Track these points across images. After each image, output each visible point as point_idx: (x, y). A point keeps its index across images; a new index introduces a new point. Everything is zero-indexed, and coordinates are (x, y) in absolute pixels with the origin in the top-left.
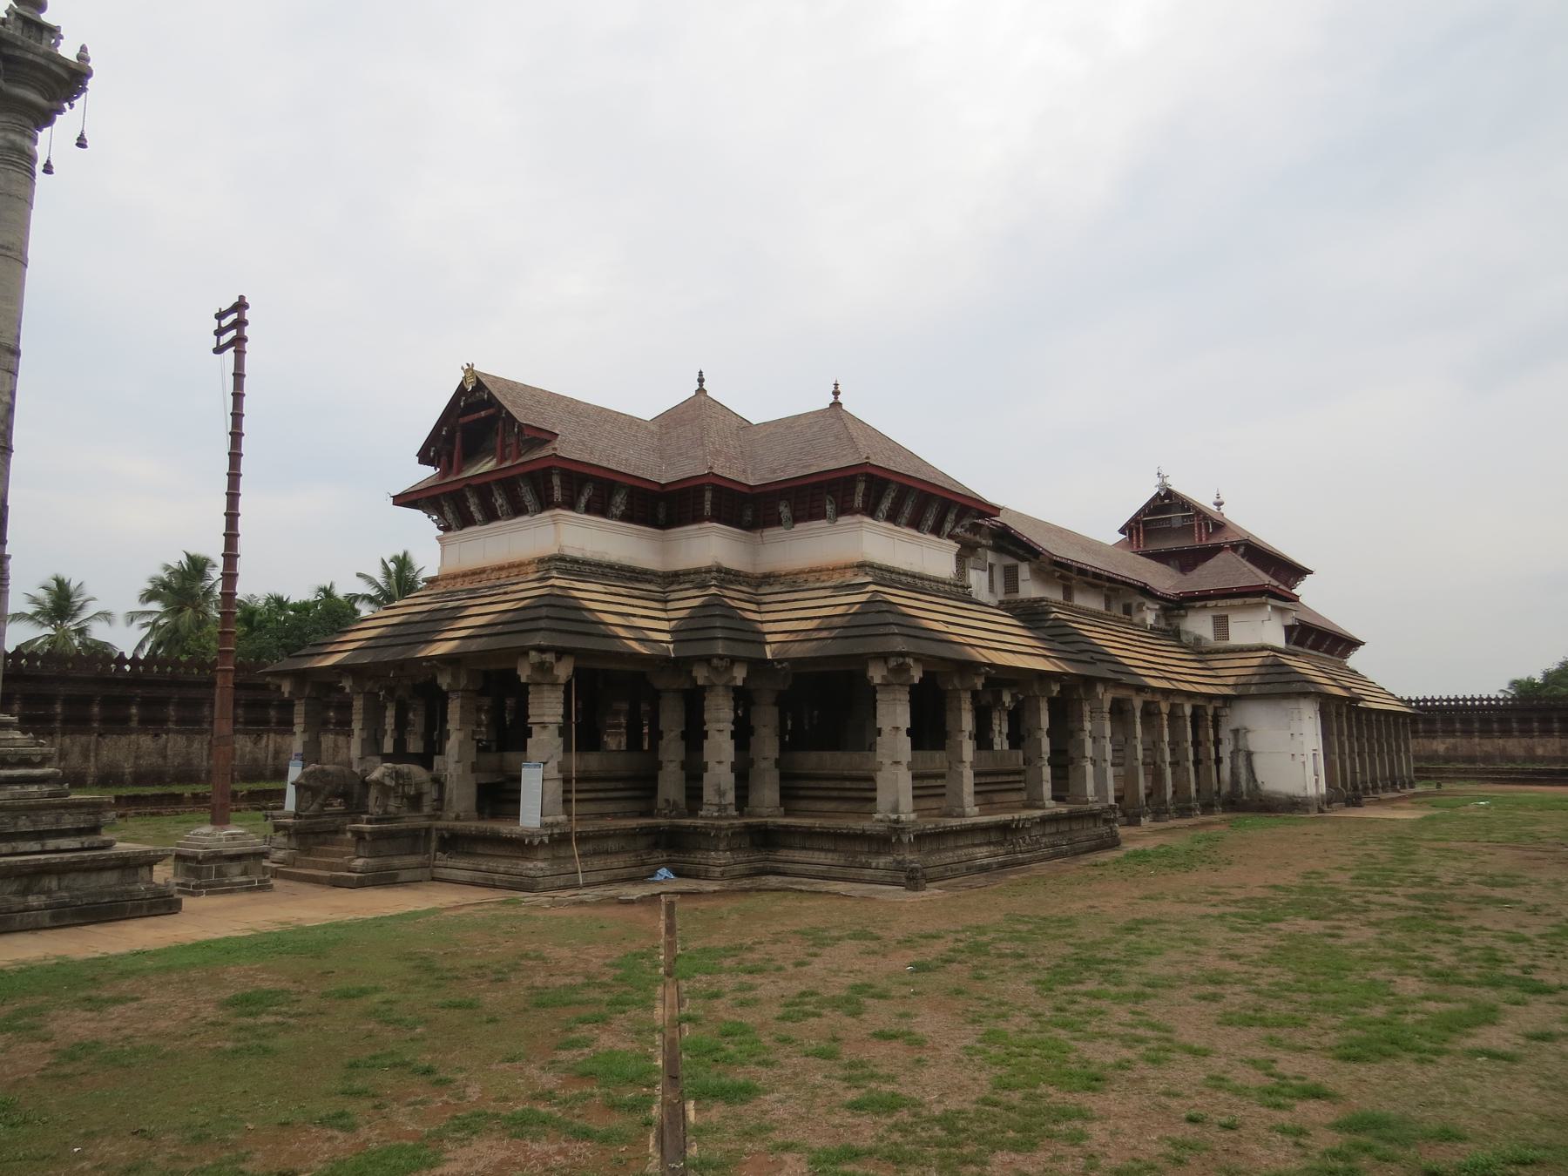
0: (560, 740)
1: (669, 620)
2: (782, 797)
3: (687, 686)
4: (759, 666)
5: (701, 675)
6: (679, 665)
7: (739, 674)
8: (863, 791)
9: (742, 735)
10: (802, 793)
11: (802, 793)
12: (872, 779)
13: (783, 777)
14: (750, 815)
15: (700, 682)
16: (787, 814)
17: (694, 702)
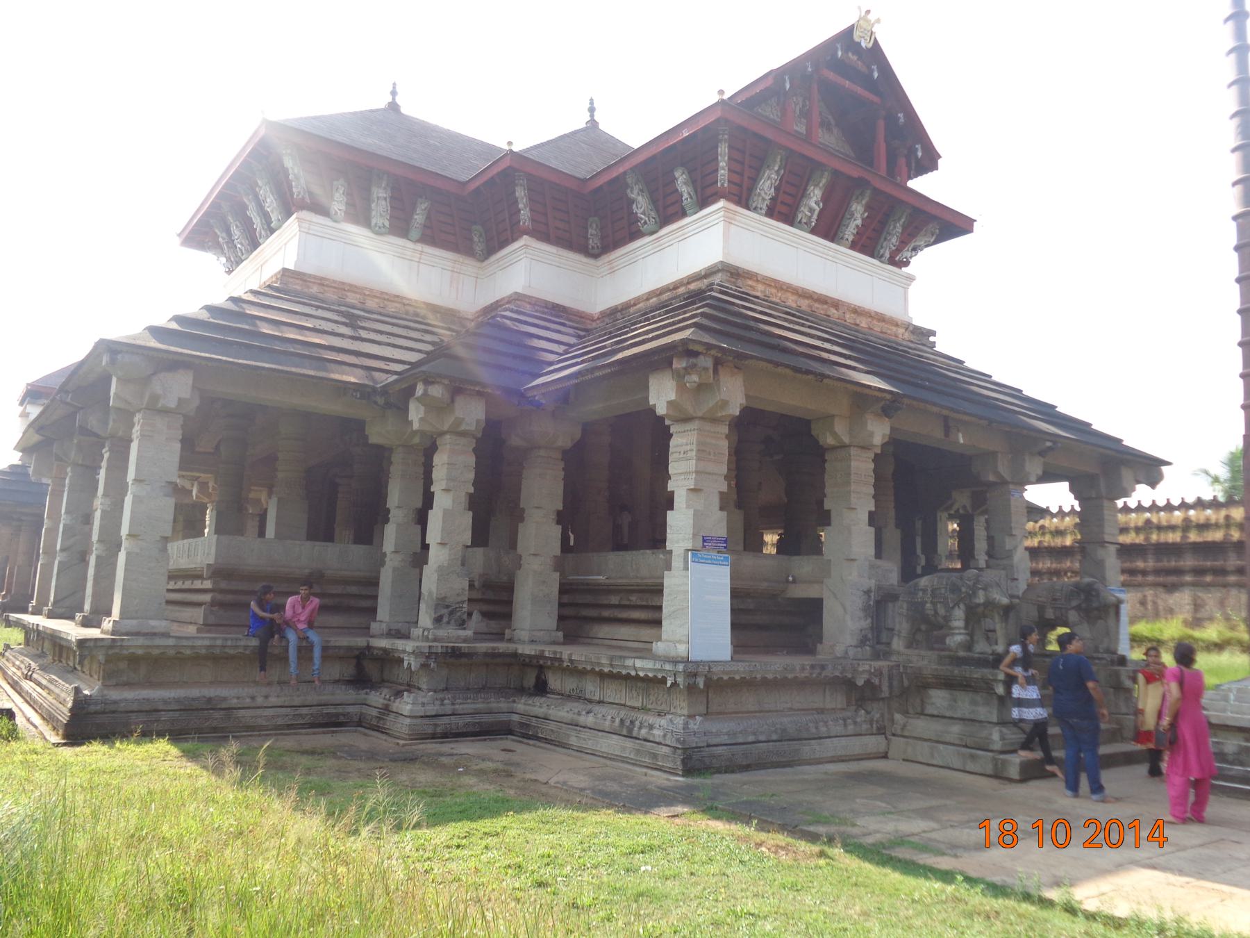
2: (561, 618)
11: (606, 613)
13: (565, 589)
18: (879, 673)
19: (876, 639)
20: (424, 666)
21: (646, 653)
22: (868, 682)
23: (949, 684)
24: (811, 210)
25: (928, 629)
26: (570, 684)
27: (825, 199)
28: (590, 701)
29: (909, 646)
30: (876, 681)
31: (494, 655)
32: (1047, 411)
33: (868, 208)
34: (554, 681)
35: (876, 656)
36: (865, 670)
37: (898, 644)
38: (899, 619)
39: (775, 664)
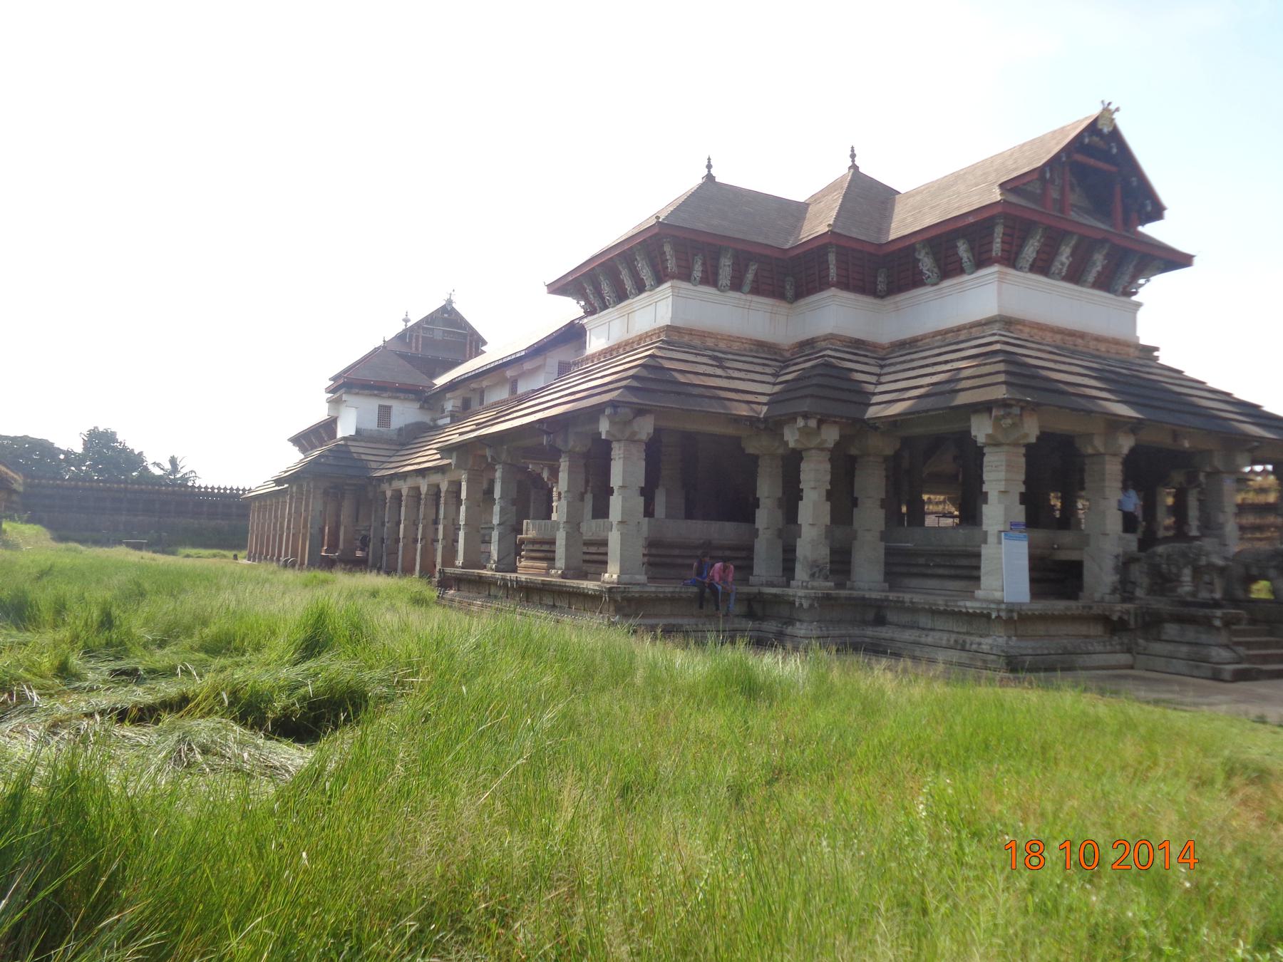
0: (642, 499)
1: (774, 384)
3: (781, 451)
4: (859, 427)
5: (791, 437)
6: (772, 426)
7: (831, 435)
8: (965, 566)
9: (843, 500)
10: (915, 570)
11: (915, 570)
12: (978, 556)
14: (851, 589)
15: (792, 445)
16: (891, 588)
17: (791, 465)
18: (1128, 612)
19: (1124, 588)
20: (811, 606)
21: (973, 598)
22: (1120, 618)
23: (1179, 619)
24: (1063, 264)
25: (1163, 582)
26: (906, 618)
27: (1073, 254)
28: (923, 629)
29: (1148, 594)
30: (1126, 617)
31: (849, 599)
32: (1252, 411)
33: (1107, 256)
34: (891, 616)
35: (1124, 600)
36: (1120, 609)
37: (1139, 593)
38: (1138, 573)
39: (1059, 606)
